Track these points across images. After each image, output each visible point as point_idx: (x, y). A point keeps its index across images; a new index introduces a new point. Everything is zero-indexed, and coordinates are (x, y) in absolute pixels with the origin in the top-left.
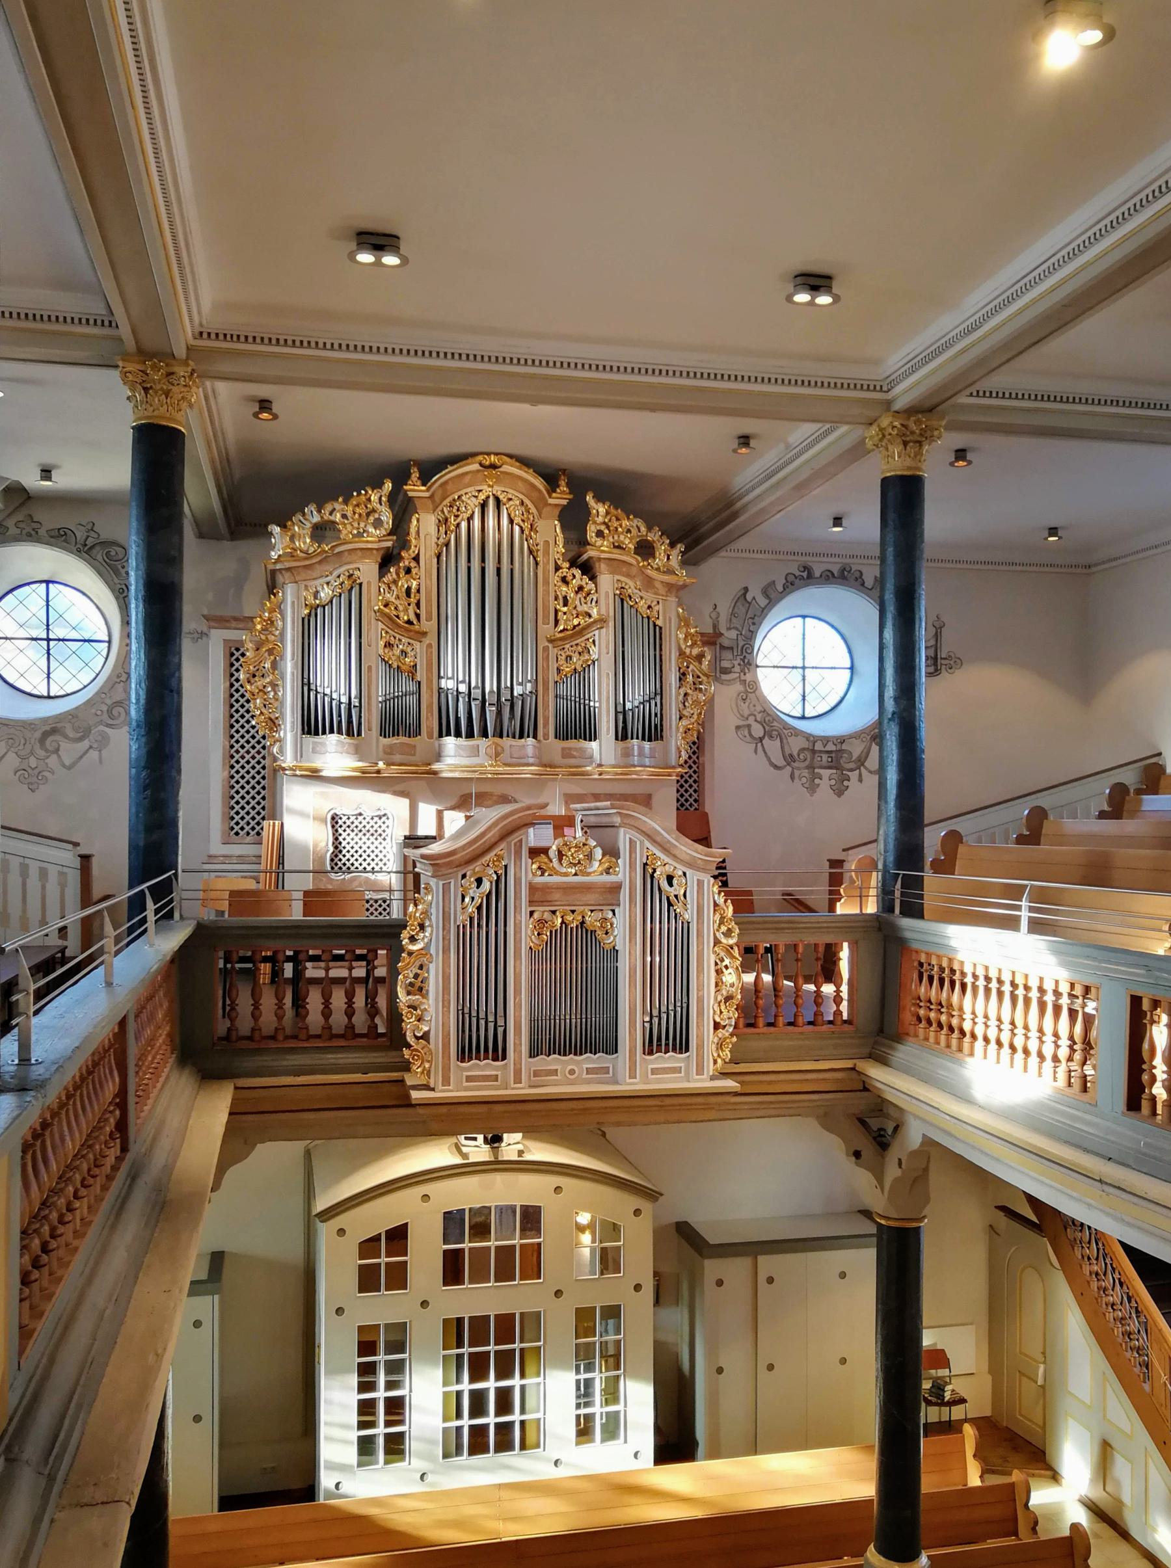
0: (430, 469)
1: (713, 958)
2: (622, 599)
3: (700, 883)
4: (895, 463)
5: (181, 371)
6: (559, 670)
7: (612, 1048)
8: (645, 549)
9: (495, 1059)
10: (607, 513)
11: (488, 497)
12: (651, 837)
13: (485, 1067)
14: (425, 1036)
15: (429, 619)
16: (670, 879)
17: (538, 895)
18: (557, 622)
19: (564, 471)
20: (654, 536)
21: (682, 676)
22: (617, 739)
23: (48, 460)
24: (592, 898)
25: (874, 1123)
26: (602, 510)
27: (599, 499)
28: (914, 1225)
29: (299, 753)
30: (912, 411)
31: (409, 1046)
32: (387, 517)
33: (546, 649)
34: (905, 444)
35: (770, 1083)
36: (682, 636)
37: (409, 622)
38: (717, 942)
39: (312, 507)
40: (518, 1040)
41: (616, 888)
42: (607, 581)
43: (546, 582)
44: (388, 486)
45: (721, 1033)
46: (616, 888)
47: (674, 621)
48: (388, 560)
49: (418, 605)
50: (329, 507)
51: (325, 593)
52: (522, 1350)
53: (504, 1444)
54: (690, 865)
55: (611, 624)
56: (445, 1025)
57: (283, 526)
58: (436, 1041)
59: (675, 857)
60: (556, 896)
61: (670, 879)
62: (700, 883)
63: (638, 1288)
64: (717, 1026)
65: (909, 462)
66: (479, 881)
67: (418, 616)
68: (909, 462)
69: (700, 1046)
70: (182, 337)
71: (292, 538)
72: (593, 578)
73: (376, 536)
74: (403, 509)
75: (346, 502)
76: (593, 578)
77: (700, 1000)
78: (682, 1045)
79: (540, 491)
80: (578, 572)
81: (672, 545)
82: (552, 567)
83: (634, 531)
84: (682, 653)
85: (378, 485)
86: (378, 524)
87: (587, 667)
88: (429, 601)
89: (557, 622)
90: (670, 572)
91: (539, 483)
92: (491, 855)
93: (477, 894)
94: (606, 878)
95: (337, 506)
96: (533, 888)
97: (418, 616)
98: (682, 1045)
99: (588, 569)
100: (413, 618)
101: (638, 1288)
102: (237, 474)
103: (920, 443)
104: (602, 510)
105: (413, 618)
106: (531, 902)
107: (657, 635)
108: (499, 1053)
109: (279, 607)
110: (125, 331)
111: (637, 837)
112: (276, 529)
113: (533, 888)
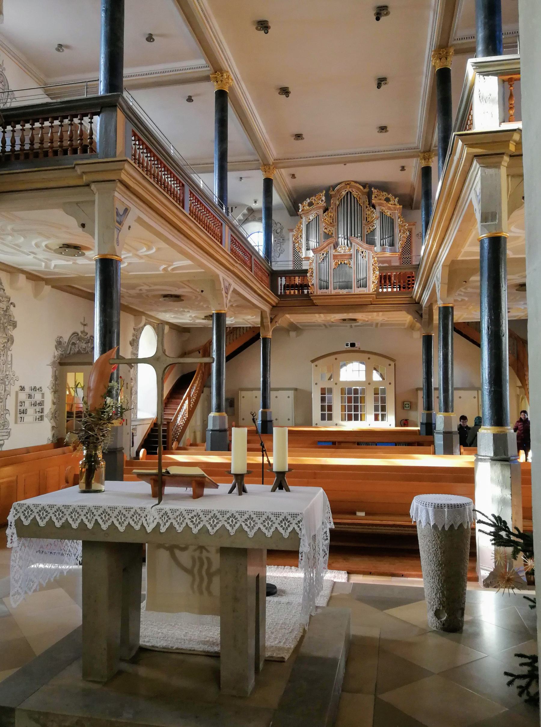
0: (334, 187)
1: (372, 268)
2: (382, 213)
3: (369, 253)
4: (424, 164)
5: (271, 167)
6: (367, 232)
7: (351, 288)
8: (388, 200)
9: (327, 289)
10: (377, 192)
11: (347, 193)
12: (357, 244)
13: (325, 290)
14: (313, 285)
15: (336, 222)
16: (362, 252)
17: (335, 257)
18: (366, 220)
19: (367, 184)
20: (390, 196)
21: (400, 231)
22: (381, 246)
23: (256, 199)
24: (346, 257)
25: (420, 312)
26: (376, 191)
27: (375, 189)
28: (430, 334)
29: (306, 254)
30: (424, 152)
31: (310, 287)
32: (324, 198)
33: (364, 226)
34: (425, 159)
35: (393, 301)
36: (399, 220)
37: (331, 223)
38: (373, 265)
39: (308, 199)
40: (331, 287)
41: (351, 255)
42: (377, 208)
43: (364, 210)
44: (324, 192)
45: (374, 284)
46: (351, 255)
47: (397, 217)
48: (326, 210)
49: (333, 219)
50: (311, 198)
51: (311, 218)
52: (361, 397)
53: (356, 419)
54: (367, 249)
55: (379, 218)
56: (317, 282)
57: (302, 204)
58: (315, 285)
59: (363, 248)
60: (339, 257)
61: (362, 252)
62: (369, 253)
63: (390, 384)
64: (373, 282)
65: (426, 164)
66: (323, 254)
67: (333, 221)
68: (426, 164)
69: (369, 286)
70: (271, 161)
71: (304, 207)
72: (375, 208)
73: (323, 204)
74: (328, 197)
75: (315, 197)
76: (375, 208)
77: (369, 277)
78: (365, 286)
79: (361, 189)
80: (372, 208)
81: (395, 198)
82: (365, 207)
83: (384, 195)
84: (400, 225)
85: (322, 192)
86: (322, 201)
87: (374, 230)
88: (335, 218)
89: (366, 220)
90: (395, 205)
91: (361, 187)
92: (325, 249)
93: (322, 257)
94: (349, 253)
95: (313, 198)
96: (334, 255)
97: (333, 221)
98: (365, 286)
99: (374, 207)
100: (331, 222)
101: (390, 384)
102: (295, 196)
103: (429, 159)
104: (376, 191)
105: (331, 222)
106: (334, 259)
107: (392, 222)
108: (327, 288)
109: (301, 223)
110: (260, 161)
111: (355, 244)
112: (300, 205)
113: (334, 255)
